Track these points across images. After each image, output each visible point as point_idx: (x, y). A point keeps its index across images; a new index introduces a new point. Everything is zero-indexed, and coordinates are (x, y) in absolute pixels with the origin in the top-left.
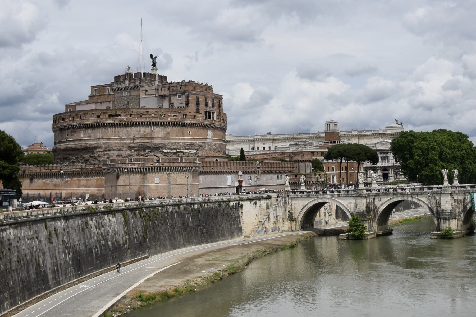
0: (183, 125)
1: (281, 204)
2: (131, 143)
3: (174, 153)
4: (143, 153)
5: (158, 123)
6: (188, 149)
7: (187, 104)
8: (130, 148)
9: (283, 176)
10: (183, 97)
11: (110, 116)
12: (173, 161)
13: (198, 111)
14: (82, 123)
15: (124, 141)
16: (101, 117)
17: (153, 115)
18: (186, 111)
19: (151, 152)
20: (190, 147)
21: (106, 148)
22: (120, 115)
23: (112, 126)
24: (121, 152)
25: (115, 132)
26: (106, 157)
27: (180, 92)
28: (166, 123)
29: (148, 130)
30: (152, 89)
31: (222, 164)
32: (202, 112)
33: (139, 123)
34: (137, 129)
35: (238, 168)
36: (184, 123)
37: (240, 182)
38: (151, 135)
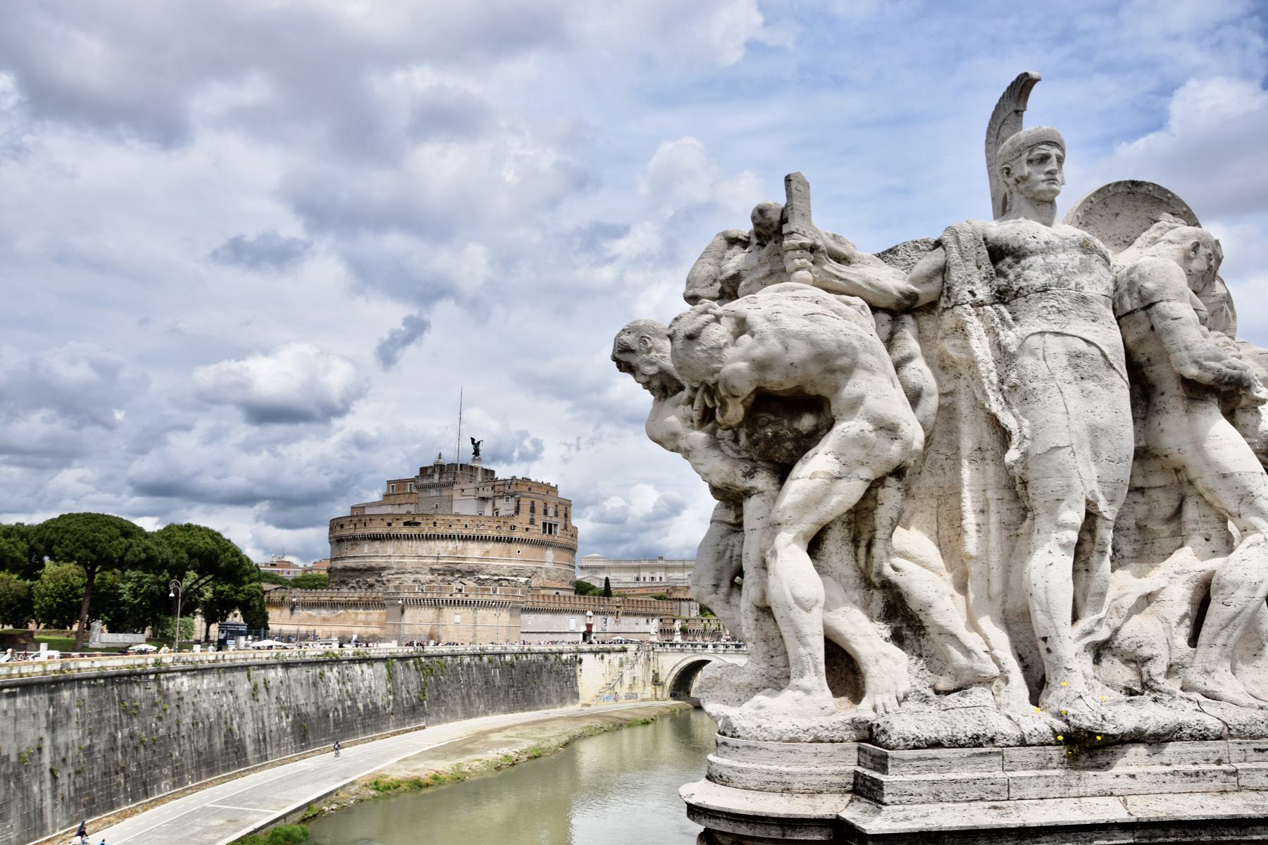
0: (510, 541)
4: (450, 578)
7: (517, 511)
8: (432, 571)
10: (512, 502)
11: (406, 524)
13: (532, 522)
29: (460, 544)
30: (470, 488)
34: (444, 544)
37: (589, 626)
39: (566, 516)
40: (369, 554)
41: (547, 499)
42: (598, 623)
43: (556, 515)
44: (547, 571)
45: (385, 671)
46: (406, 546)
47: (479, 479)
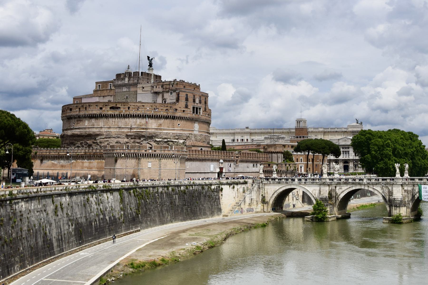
0: (174, 118)
1: (256, 188)
2: (128, 132)
3: (165, 142)
4: (138, 141)
5: (153, 115)
6: (177, 139)
7: (178, 100)
8: (127, 136)
9: (258, 165)
10: (174, 94)
11: (111, 108)
12: (163, 149)
13: (186, 107)
14: (87, 113)
16: (104, 109)
17: (148, 108)
19: (145, 140)
20: (179, 137)
21: (107, 135)
22: (120, 108)
23: (113, 117)
24: (119, 139)
25: (114, 122)
26: (106, 143)
27: (172, 90)
28: (159, 116)
29: (143, 121)
31: (206, 153)
32: (191, 107)
33: (136, 115)
34: (134, 120)
35: (220, 157)
36: (175, 116)
37: (221, 169)
38: (146, 126)
40: (87, 126)
41: (195, 92)
42: (226, 167)
44: (195, 136)
46: (111, 121)
47: (152, 81)
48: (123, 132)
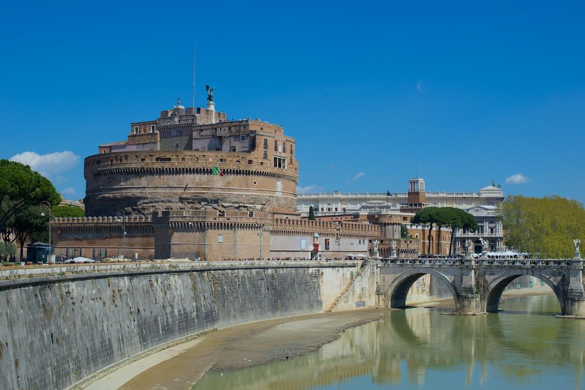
0: (248, 173)
2: (183, 194)
3: (236, 208)
4: (198, 206)
6: (252, 204)
8: (181, 200)
11: (157, 159)
13: (265, 156)
15: (175, 191)
17: (211, 160)
18: (253, 156)
20: (256, 200)
25: (163, 179)
28: (227, 170)
33: (193, 169)
35: (314, 229)
36: (249, 171)
37: (316, 246)
39: (291, 153)
43: (284, 151)
44: (278, 199)
45: (190, 281)
48: (175, 194)
